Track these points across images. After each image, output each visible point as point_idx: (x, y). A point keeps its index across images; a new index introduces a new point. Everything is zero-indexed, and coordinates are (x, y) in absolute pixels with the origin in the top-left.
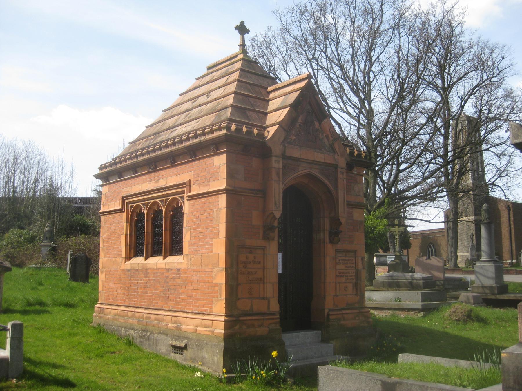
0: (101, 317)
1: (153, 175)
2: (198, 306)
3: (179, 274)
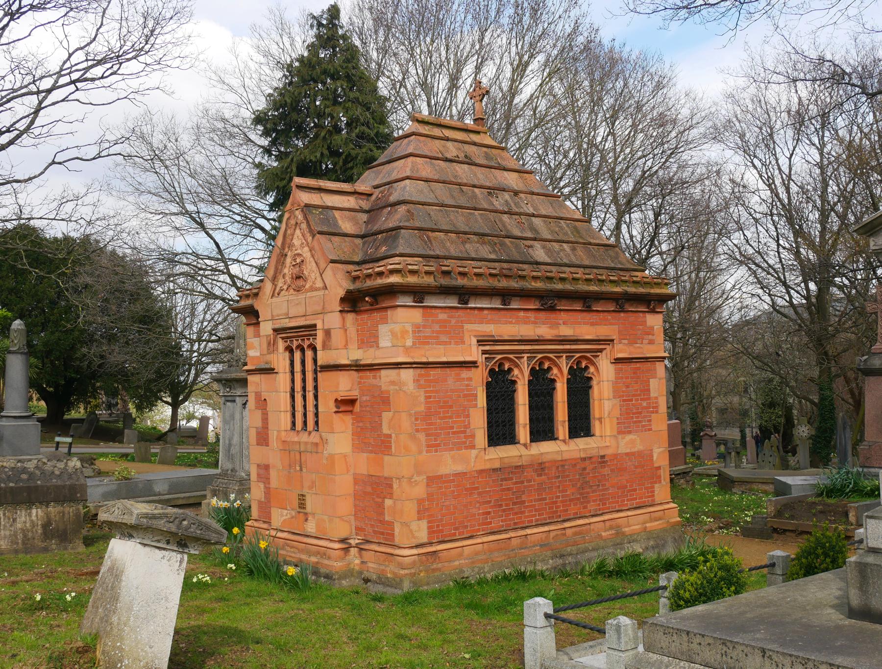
0: (434, 570)
1: (542, 315)
2: (636, 499)
3: (604, 462)
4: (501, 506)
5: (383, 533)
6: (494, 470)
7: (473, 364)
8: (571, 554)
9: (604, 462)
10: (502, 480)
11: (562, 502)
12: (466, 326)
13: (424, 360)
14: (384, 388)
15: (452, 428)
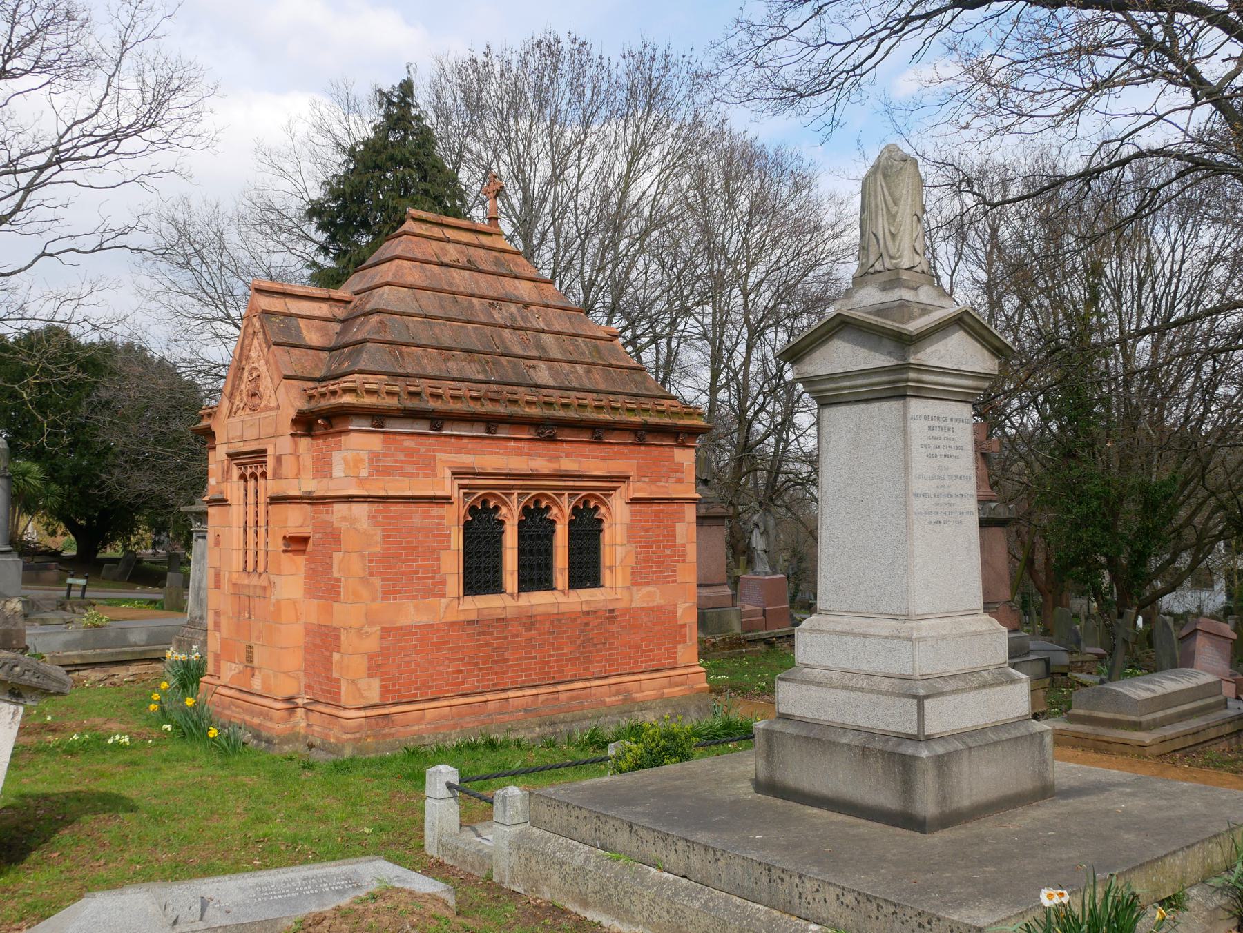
0: (385, 736)
1: (539, 446)
3: (613, 617)
4: (477, 664)
5: (329, 692)
6: (470, 623)
7: (446, 500)
8: (563, 722)
9: (613, 617)
10: (479, 634)
11: (557, 661)
12: (439, 456)
13: (382, 493)
14: (336, 525)
15: (417, 572)
